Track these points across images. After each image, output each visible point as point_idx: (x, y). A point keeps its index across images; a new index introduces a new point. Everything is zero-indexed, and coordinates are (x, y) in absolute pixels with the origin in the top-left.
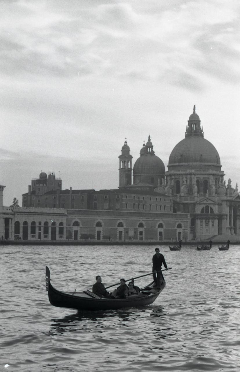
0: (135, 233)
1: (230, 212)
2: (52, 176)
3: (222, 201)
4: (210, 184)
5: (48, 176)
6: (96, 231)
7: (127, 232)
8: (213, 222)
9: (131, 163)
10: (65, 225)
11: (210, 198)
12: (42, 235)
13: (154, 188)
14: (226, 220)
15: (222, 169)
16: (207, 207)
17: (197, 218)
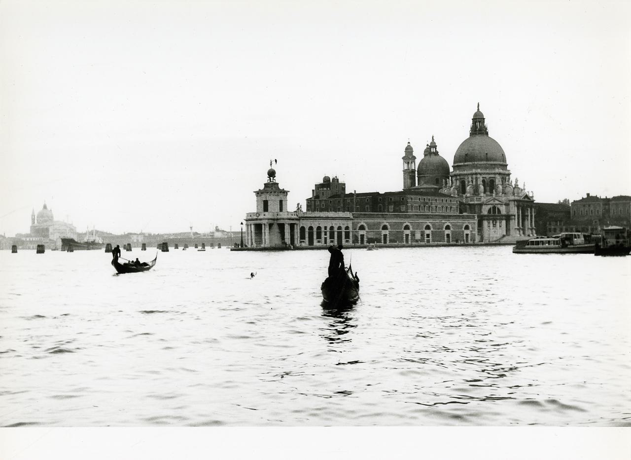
0: (422, 235)
1: (518, 212)
2: (336, 180)
3: (510, 201)
4: (497, 184)
5: (331, 180)
6: (382, 235)
7: (413, 234)
8: (500, 223)
9: (415, 164)
10: (351, 229)
11: (496, 198)
12: (328, 240)
13: (439, 189)
14: (514, 220)
15: (508, 168)
16: (494, 208)
17: (484, 220)
